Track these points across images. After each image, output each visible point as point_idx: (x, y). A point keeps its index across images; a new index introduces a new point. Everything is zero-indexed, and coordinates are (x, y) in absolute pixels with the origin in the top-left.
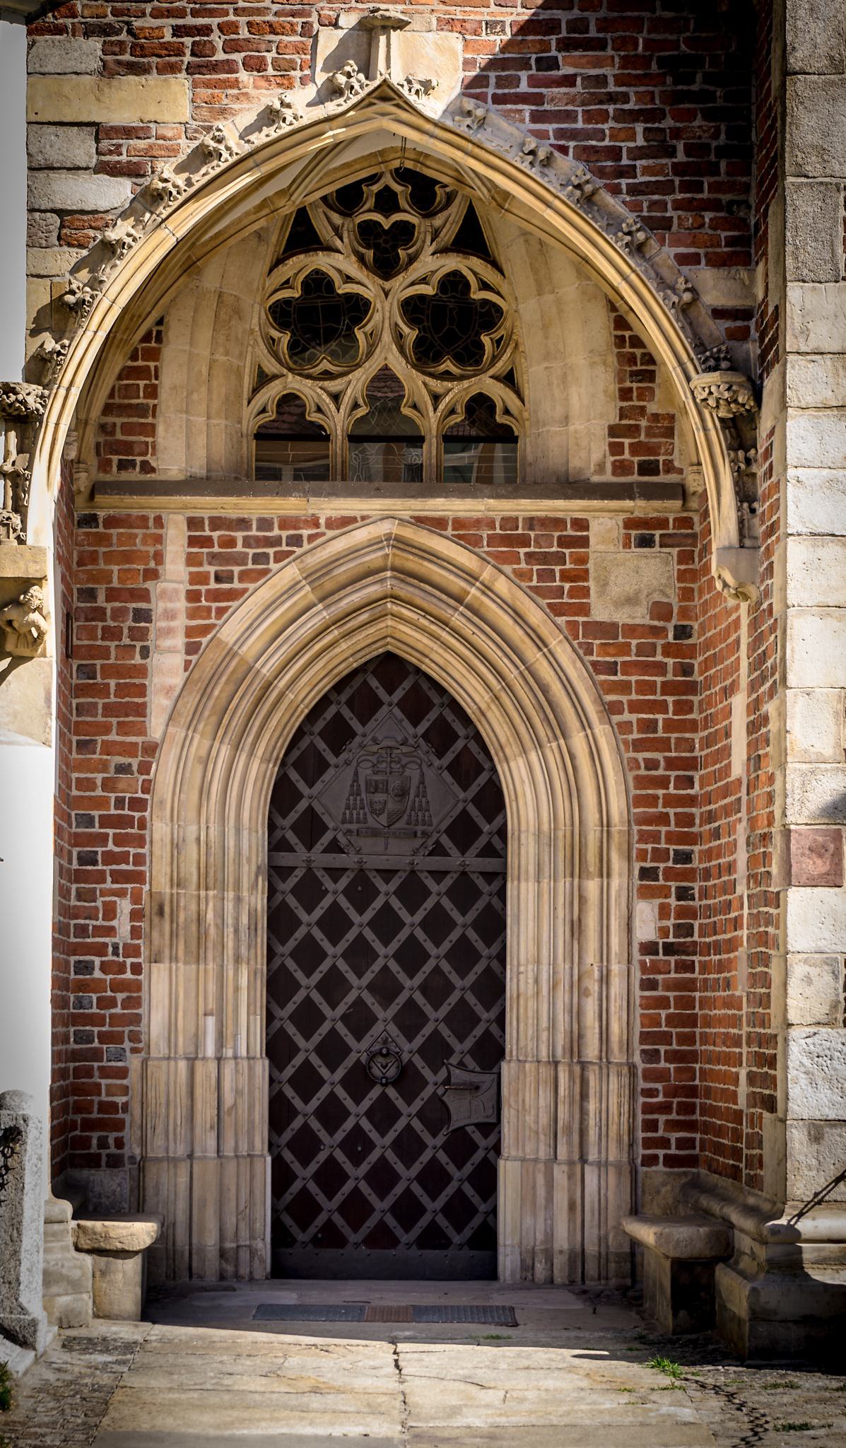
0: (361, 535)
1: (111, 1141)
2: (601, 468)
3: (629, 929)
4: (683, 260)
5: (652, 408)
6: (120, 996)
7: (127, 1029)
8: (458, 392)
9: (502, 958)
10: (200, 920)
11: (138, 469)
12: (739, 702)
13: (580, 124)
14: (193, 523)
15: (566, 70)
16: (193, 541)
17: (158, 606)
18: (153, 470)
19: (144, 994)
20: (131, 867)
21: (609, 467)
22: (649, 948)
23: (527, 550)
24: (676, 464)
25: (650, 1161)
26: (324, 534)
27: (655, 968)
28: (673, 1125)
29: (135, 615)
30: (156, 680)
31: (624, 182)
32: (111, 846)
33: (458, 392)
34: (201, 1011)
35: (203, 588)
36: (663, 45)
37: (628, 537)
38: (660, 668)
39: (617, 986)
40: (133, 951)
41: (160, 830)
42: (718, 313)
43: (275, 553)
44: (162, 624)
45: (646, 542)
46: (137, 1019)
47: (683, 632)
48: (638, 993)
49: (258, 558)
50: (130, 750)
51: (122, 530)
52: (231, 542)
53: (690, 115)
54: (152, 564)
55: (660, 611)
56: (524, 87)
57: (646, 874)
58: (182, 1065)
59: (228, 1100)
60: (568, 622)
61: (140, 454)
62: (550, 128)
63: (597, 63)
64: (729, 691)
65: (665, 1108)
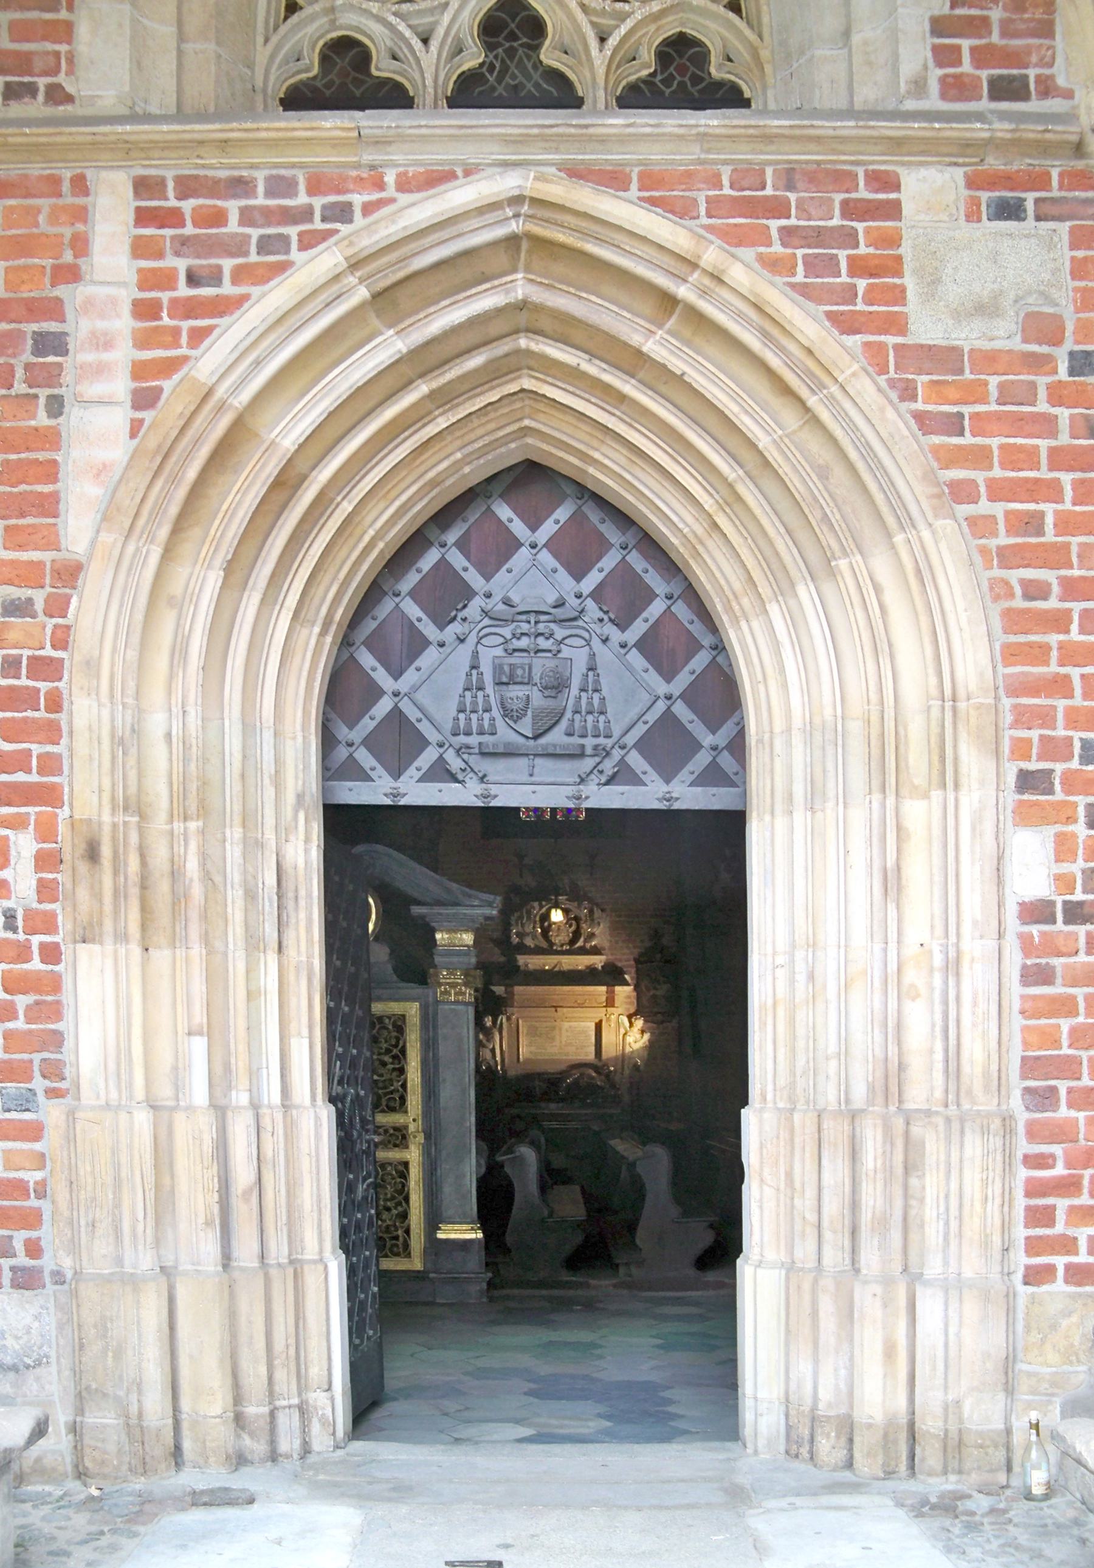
1: (18, 1245)
2: (919, 87)
6: (22, 1001)
7: (37, 1058)
11: (41, 97)
14: (143, 186)
16: (143, 217)
18: (69, 99)
19: (66, 997)
20: (34, 778)
21: (934, 87)
23: (784, 222)
24: (1061, 81)
26: (393, 200)
29: (35, 341)
30: (75, 453)
34: (182, 1028)
35: (165, 296)
37: (975, 203)
43: (300, 235)
44: (88, 357)
45: (1008, 211)
46: (56, 1040)
49: (265, 245)
50: (31, 575)
51: (12, 202)
52: (219, 218)
54: (68, 257)
60: (867, 345)
61: (46, 73)
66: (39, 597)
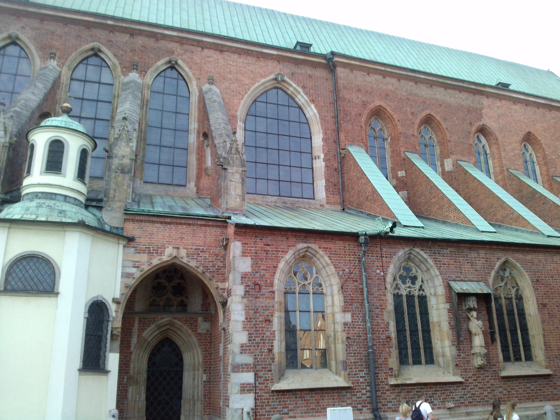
0: (164, 320)
3: (202, 378)
4: (218, 282)
5: (207, 302)
8: (179, 299)
9: (182, 383)
10: (137, 379)
12: (221, 346)
13: (203, 263)
14: (140, 318)
15: (201, 255)
16: (139, 321)
17: (134, 331)
22: (205, 382)
25: (204, 415)
27: (206, 385)
28: (208, 409)
31: (209, 271)
32: (124, 368)
33: (179, 299)
36: (214, 252)
38: (207, 340)
39: (200, 388)
40: (126, 384)
41: (132, 365)
42: (221, 289)
46: (126, 395)
47: (211, 334)
48: (203, 389)
50: (128, 353)
53: (218, 262)
55: (208, 331)
56: (195, 257)
57: (205, 370)
58: (133, 402)
59: (140, 407)
62: (199, 263)
63: (205, 254)
64: (220, 343)
65: (207, 406)
66: (128, 355)
